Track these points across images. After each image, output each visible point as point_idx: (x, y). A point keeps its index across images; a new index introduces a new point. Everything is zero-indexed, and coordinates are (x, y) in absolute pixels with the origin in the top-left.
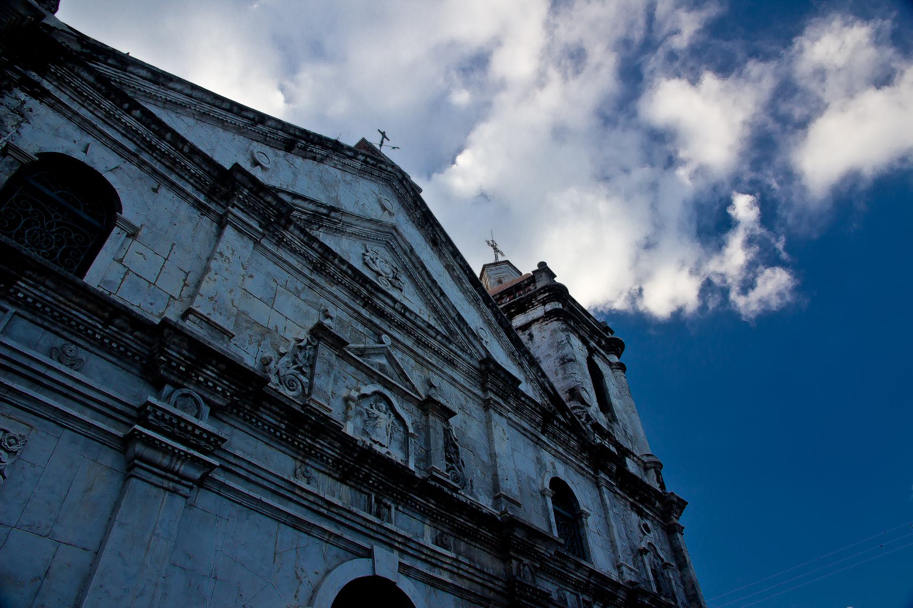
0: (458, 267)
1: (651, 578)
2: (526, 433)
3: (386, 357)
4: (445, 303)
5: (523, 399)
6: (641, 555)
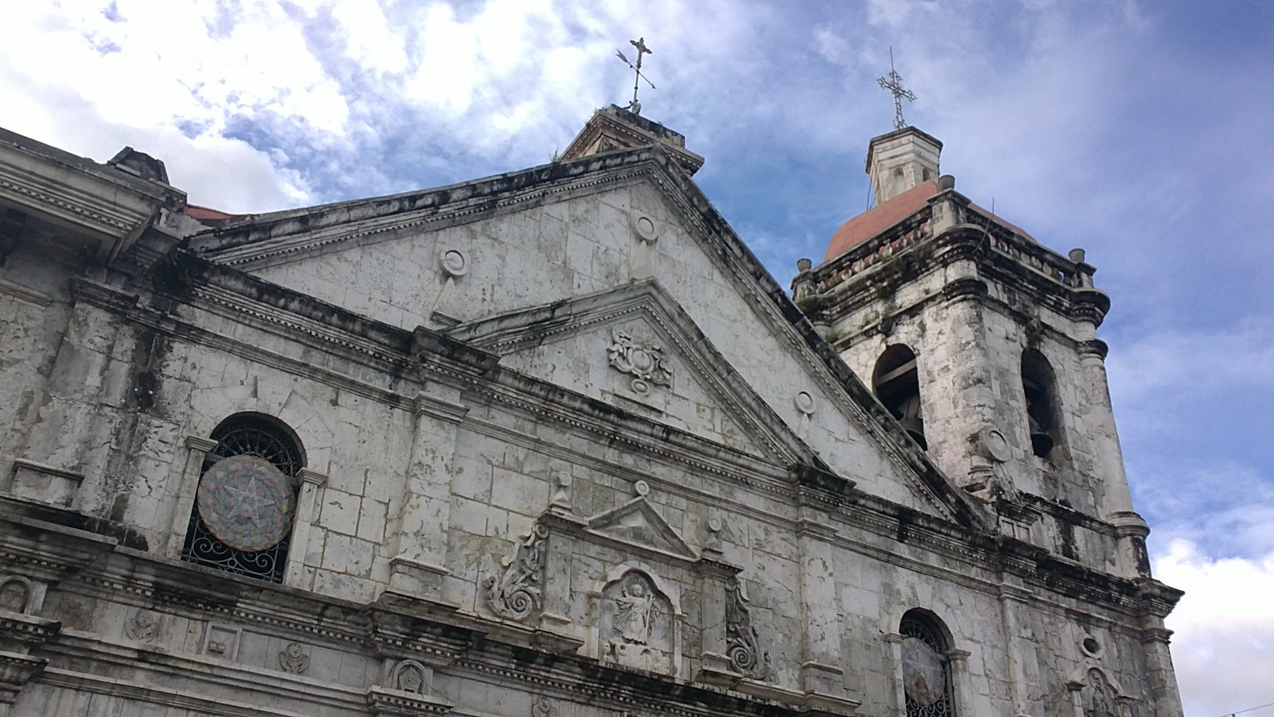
2: (869, 552)
3: (643, 513)
4: (734, 385)
5: (862, 502)
6: (1070, 691)
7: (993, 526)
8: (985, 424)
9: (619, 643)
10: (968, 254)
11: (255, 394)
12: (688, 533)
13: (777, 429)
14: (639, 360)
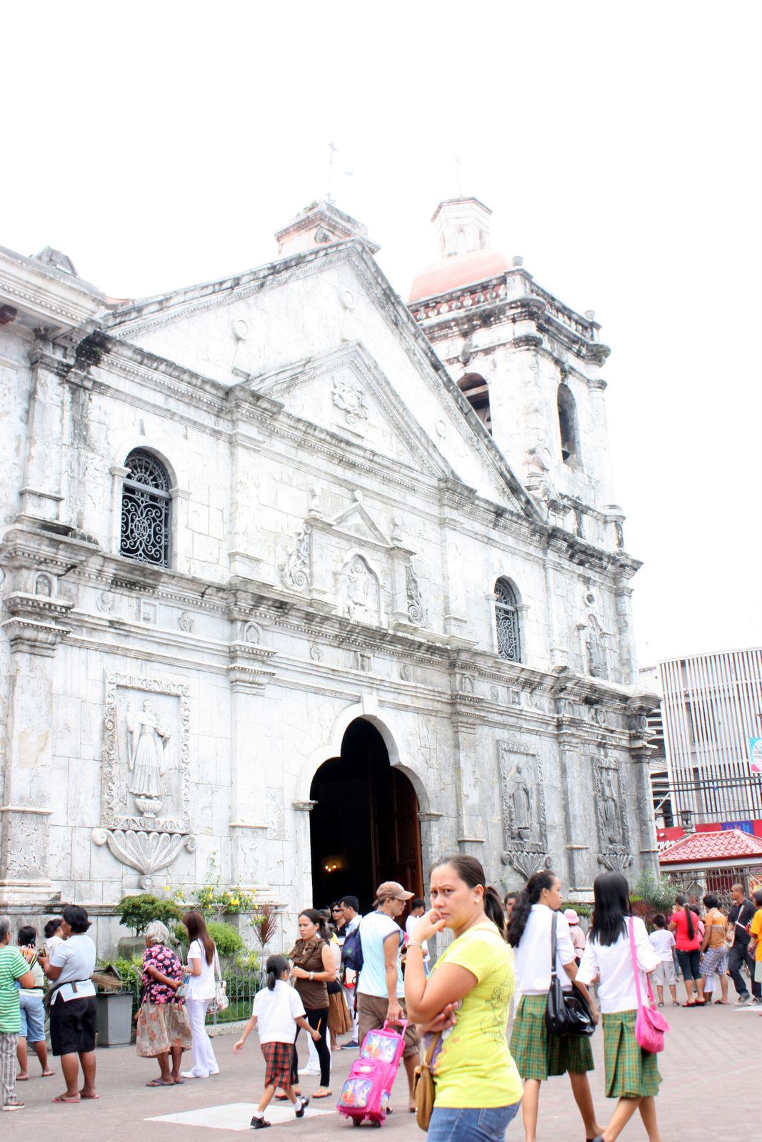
0: (421, 351)
1: (584, 652)
2: (478, 537)
4: (406, 418)
7: (545, 518)
8: (539, 442)
9: (352, 606)
10: (532, 316)
11: (143, 432)
12: (384, 528)
13: (431, 450)
14: (350, 400)
